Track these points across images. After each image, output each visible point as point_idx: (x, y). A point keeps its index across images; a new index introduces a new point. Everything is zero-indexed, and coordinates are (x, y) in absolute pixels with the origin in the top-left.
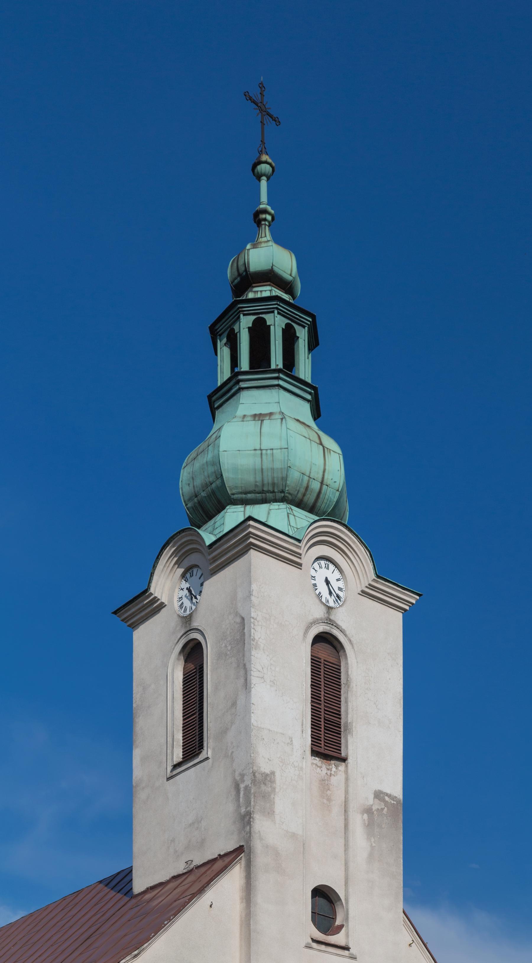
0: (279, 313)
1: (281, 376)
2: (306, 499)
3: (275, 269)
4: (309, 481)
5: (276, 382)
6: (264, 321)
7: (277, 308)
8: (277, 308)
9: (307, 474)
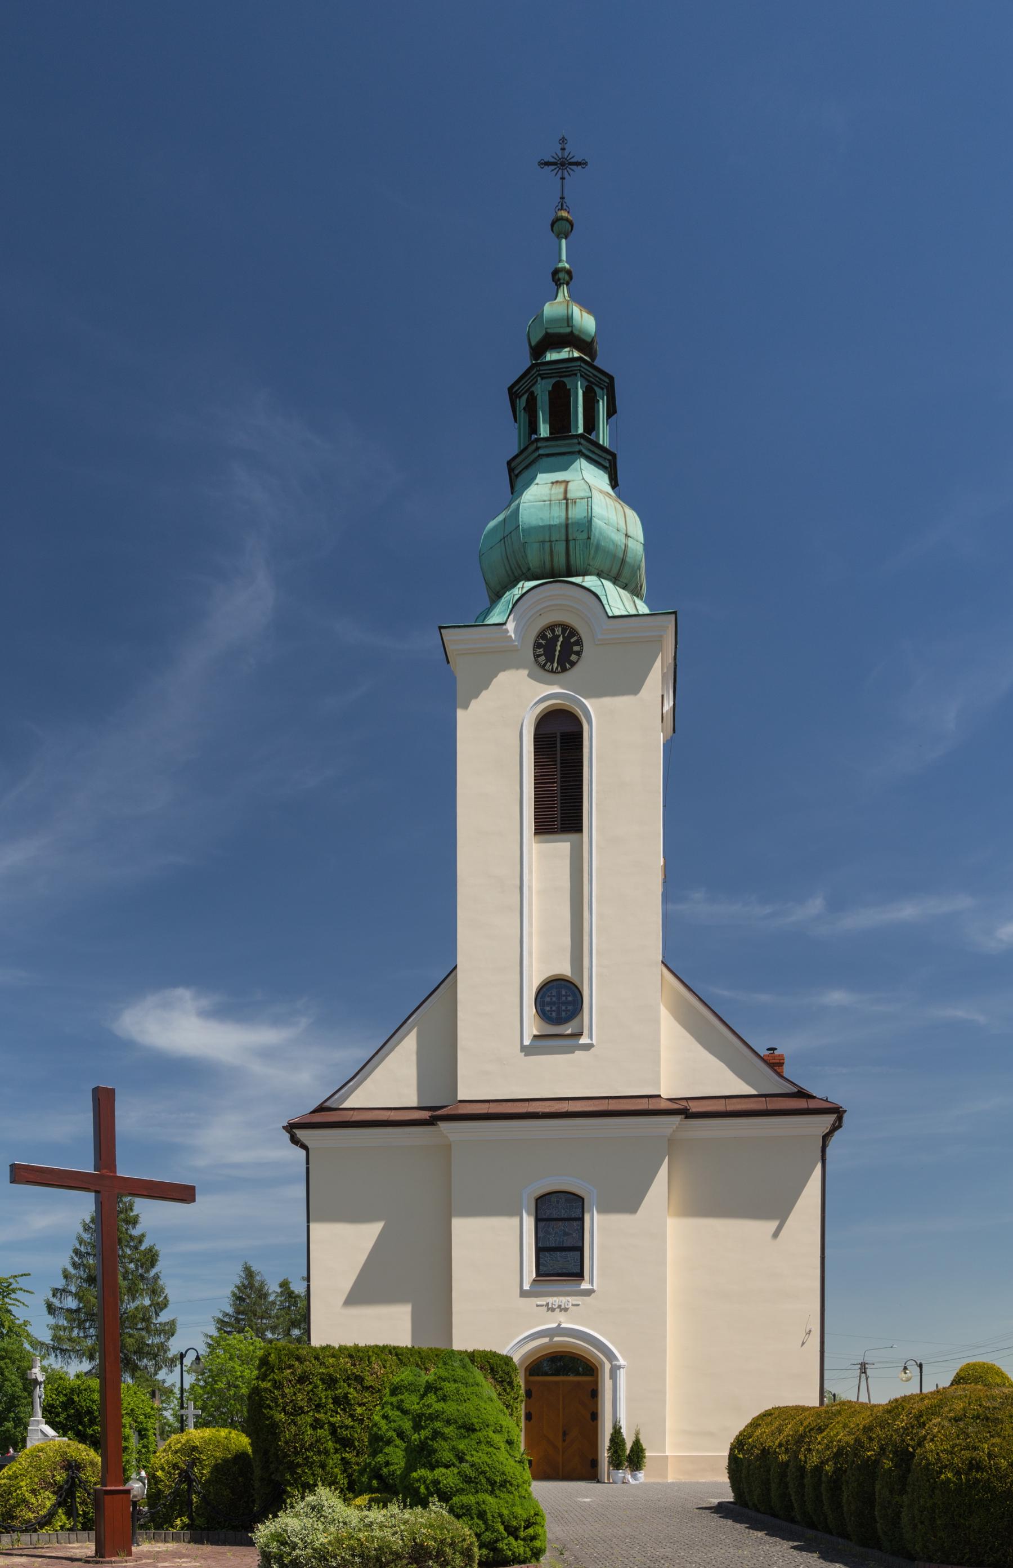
0: (542, 379)
1: (539, 444)
2: (556, 565)
3: (550, 331)
4: (551, 546)
5: (536, 454)
6: (564, 384)
7: (540, 375)
8: (540, 375)
9: (547, 539)
